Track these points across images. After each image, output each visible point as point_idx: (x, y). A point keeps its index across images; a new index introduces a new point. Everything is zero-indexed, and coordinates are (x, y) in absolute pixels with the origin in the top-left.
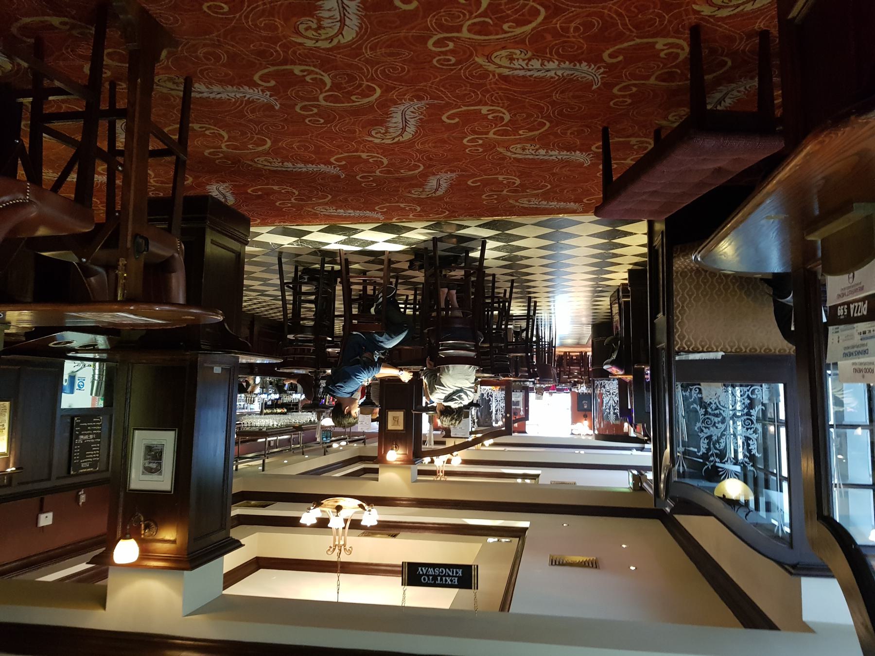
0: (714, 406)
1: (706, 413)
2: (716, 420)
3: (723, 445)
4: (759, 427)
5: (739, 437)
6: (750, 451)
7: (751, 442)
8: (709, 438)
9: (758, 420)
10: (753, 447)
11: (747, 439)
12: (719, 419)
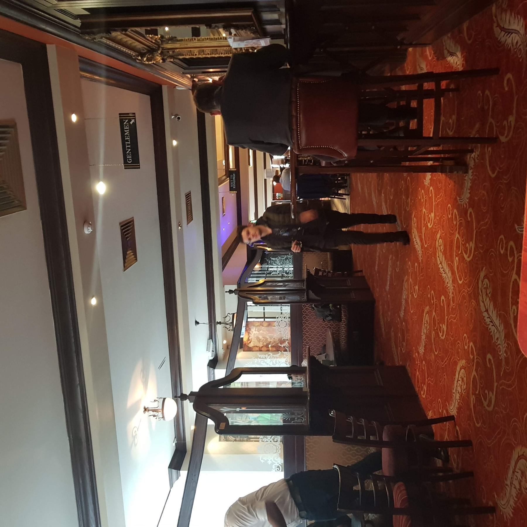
0: (286, 262)
1: (284, 260)
3: (274, 264)
4: (280, 275)
5: (276, 269)
6: (273, 272)
7: (275, 272)
10: (274, 273)
11: (276, 271)
12: (282, 264)
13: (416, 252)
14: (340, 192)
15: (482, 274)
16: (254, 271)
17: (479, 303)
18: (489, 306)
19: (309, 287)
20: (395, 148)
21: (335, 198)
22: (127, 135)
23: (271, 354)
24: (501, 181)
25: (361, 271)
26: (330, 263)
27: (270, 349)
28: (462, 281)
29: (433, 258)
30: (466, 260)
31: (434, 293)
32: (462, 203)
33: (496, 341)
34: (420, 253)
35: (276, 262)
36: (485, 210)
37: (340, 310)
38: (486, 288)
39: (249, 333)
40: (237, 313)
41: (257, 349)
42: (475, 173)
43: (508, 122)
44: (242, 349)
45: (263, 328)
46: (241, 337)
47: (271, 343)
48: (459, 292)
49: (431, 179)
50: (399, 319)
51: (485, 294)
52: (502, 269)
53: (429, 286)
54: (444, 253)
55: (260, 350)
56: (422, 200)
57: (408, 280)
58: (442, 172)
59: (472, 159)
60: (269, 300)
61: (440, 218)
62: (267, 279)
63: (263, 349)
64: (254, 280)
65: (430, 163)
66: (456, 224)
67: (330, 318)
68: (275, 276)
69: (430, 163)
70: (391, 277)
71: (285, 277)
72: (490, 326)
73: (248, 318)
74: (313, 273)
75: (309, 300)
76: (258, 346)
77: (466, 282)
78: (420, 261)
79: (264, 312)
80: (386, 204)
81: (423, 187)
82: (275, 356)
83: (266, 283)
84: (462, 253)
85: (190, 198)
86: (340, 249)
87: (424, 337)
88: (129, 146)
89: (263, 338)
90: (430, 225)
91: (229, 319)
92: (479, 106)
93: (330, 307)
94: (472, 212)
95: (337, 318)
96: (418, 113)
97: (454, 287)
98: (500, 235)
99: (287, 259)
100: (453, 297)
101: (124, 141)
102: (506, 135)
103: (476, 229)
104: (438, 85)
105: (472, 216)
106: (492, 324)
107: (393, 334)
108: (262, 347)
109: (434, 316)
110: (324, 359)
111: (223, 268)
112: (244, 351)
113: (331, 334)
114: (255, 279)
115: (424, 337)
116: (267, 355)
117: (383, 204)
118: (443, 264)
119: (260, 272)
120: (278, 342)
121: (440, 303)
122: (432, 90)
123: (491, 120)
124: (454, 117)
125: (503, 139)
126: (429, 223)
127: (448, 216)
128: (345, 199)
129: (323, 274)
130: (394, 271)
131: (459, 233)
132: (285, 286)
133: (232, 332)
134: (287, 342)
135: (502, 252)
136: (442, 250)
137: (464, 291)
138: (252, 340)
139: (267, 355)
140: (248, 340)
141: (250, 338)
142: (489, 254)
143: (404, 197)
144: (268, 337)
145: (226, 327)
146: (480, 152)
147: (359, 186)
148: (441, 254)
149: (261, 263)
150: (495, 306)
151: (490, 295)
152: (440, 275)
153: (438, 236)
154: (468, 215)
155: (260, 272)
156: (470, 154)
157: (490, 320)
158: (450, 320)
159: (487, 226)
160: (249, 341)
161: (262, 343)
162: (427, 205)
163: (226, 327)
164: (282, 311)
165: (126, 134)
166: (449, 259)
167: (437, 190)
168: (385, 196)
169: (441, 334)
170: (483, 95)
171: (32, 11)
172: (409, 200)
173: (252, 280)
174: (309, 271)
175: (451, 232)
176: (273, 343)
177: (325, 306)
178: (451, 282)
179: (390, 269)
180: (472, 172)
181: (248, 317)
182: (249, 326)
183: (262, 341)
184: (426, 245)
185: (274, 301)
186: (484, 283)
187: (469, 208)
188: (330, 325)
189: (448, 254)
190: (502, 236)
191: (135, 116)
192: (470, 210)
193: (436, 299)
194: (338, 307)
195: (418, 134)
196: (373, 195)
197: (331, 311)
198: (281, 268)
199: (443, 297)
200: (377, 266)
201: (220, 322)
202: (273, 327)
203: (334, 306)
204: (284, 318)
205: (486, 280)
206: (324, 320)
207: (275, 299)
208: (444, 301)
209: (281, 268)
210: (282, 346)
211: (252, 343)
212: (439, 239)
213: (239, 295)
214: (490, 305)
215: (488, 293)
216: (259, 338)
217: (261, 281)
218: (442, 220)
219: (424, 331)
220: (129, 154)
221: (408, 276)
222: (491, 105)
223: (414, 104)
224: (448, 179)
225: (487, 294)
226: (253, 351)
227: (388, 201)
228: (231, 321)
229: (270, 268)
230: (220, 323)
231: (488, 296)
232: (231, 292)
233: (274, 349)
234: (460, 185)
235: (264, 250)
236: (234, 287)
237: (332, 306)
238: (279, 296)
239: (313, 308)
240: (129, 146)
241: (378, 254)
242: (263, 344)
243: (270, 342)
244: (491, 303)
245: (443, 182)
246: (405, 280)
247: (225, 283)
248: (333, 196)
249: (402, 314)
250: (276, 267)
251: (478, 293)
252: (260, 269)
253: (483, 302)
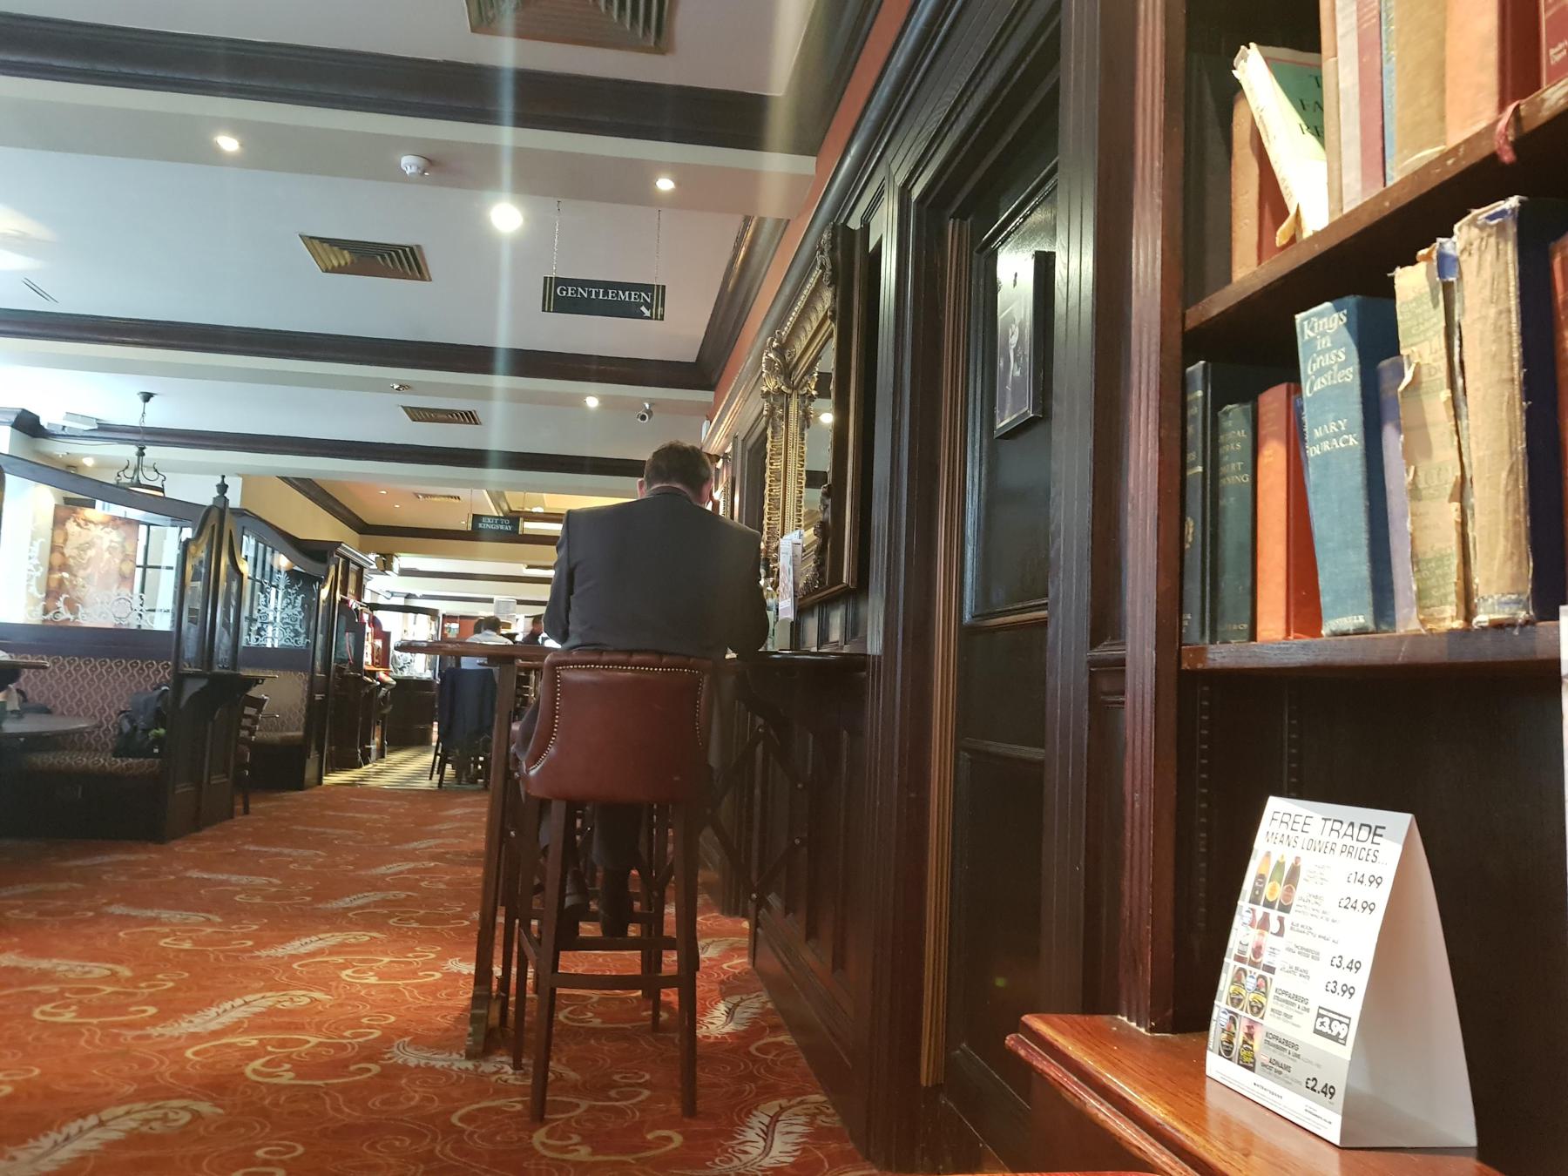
0: (288, 630)
1: (293, 626)
2: (287, 620)
3: (285, 602)
4: (256, 614)
6: (266, 597)
8: (294, 607)
9: (256, 620)
11: (266, 606)
13: (282, 943)
14: (449, 767)
15: (205, 1107)
16: (273, 552)
19: (216, 680)
20: (540, 889)
21: (436, 754)
22: (617, 294)
23: (39, 574)
24: (440, 1138)
25: (246, 811)
26: (276, 736)
27: (57, 576)
28: (191, 1057)
29: (262, 984)
30: (247, 1064)
31: (169, 990)
32: (395, 1049)
34: (280, 951)
35: (290, 607)
36: (373, 1105)
37: (147, 753)
38: (165, 1119)
39: (105, 524)
40: (164, 497)
41: (59, 541)
42: (464, 1076)
43: (576, 1145)
44: (62, 502)
45: (118, 561)
46: (99, 503)
47: (73, 578)
48: (162, 1052)
49: (459, 974)
50: (104, 901)
52: (215, 1154)
53: (187, 975)
54: (272, 1012)
55: (53, 549)
56: (410, 955)
57: (209, 922)
58: (475, 998)
59: (500, 1067)
60: (190, 584)
61: (362, 999)
62: (247, 584)
63: (57, 556)
64: (247, 549)
65: (497, 971)
66: (345, 1037)
67: (126, 727)
68: (255, 603)
69: (497, 971)
70: (222, 883)
71: (250, 625)
72: (54, 1136)
73: (149, 525)
74: (254, 692)
75: (180, 679)
76: (68, 543)
77: (188, 1068)
78: (257, 953)
79: (159, 567)
80: (410, 871)
81: (442, 957)
82: (33, 582)
83: (236, 575)
85: (465, 422)
86: (308, 761)
87: (45, 964)
88: (593, 296)
89: (87, 557)
91: (148, 477)
92: (617, 1077)
93: (157, 729)
94: (369, 1075)
95: (126, 745)
96: (613, 939)
97: (179, 1038)
98: (304, 1144)
99: (297, 634)
100: (148, 1037)
101: (607, 285)
102: (546, 1141)
103: (326, 1084)
104: (669, 982)
105: (361, 1075)
107: (63, 886)
108: (63, 554)
109: (97, 990)
110: (9, 708)
111: (284, 479)
112: (56, 506)
113: (79, 729)
114: (251, 554)
115: (45, 964)
116: (36, 562)
117: (411, 865)
118: (243, 1008)
119: (268, 568)
120: (74, 594)
121: (137, 1004)
122: (660, 971)
123: (584, 1105)
124: (597, 1022)
125: (539, 1136)
126: (354, 972)
127: (365, 1017)
128: (431, 779)
129: (249, 716)
130: (238, 889)
131: (320, 1044)
132: (225, 625)
133: (113, 482)
134: (68, 615)
135: (260, 1153)
136: (279, 1006)
137: (162, 1063)
138: (84, 532)
139: (36, 562)
140: (87, 521)
141: (91, 526)
142: (257, 1122)
143: (422, 912)
144: (89, 571)
145: (127, 467)
146: (514, 1085)
147: (458, 811)
148: (270, 1003)
149: (290, 573)
150: (111, 1145)
151: (145, 1129)
153: (317, 995)
154: (362, 1065)
155: (268, 568)
156: (511, 1062)
158: (89, 1030)
159: (331, 1113)
160: (82, 523)
161: (73, 554)
162: (397, 968)
163: (127, 467)
164: (157, 614)
165: (620, 292)
166: (255, 1024)
167: (432, 990)
168: (427, 870)
169: (48, 1008)
170: (640, 1084)
171: (884, 133)
172: (415, 925)
173: (248, 545)
174: (257, 683)
175: (326, 1025)
176: (71, 581)
177: (159, 718)
178: (192, 1030)
179: (244, 879)
180: (467, 1069)
181: (151, 527)
182: (127, 528)
183: (80, 555)
184: (299, 966)
185: (188, 592)
186: (179, 1113)
187: (382, 1066)
188: (108, 729)
189: (267, 1021)
190: (300, 1150)
191: (656, 319)
192: (375, 1068)
193: (151, 994)
194: (156, 751)
195: (568, 939)
196: (433, 842)
197: (146, 731)
198: (275, 618)
199: (152, 1010)
200: (257, 848)
201: (144, 454)
202: (116, 586)
203: (159, 741)
204: (140, 615)
205: (185, 1117)
206: (122, 712)
207: (192, 600)
208: (143, 1015)
209: (275, 618)
210: (60, 604)
211: (78, 529)
212: (310, 998)
213: (210, 509)
215: (154, 1124)
216: (89, 548)
217: (245, 568)
218: (356, 1003)
219: (61, 966)
220: (577, 292)
221: (220, 924)
222: (617, 1104)
223: (633, 931)
224: (456, 1014)
226: (53, 530)
227: (417, 877)
228: (143, 481)
229: (277, 592)
230: (141, 454)
231: (142, 1125)
232: (223, 488)
233: (54, 584)
234: (441, 1043)
235: (322, 582)
236: (234, 499)
237: (157, 736)
238: (198, 606)
239: (159, 687)
240: (593, 296)
241: (286, 851)
242: (70, 557)
243: (75, 576)
245: (449, 1004)
246: (211, 917)
247: (248, 479)
248: (439, 752)
249: (117, 910)
250: (279, 608)
251: (153, 1100)
252: (276, 568)
253: (128, 1113)
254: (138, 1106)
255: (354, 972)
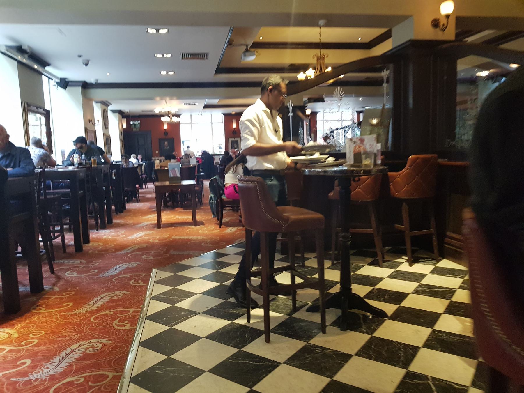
17: (77, 342)
18: (77, 353)
33: (45, 367)
38: (93, 347)
51: (88, 347)
77: (94, 325)
84: (119, 317)
90: (132, 283)
106: (61, 360)
152: (90, 298)
157: (64, 356)
212: (123, 293)
214: (79, 353)
215: (91, 349)
225: (88, 348)
231: (86, 350)
244: (81, 354)
254: (83, 343)
255: (134, 281)
